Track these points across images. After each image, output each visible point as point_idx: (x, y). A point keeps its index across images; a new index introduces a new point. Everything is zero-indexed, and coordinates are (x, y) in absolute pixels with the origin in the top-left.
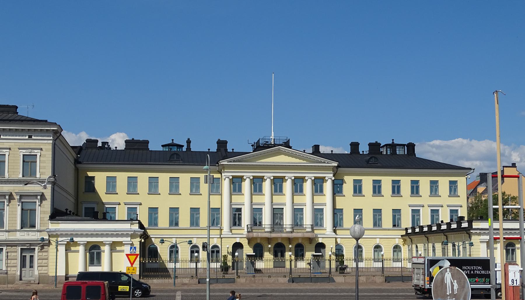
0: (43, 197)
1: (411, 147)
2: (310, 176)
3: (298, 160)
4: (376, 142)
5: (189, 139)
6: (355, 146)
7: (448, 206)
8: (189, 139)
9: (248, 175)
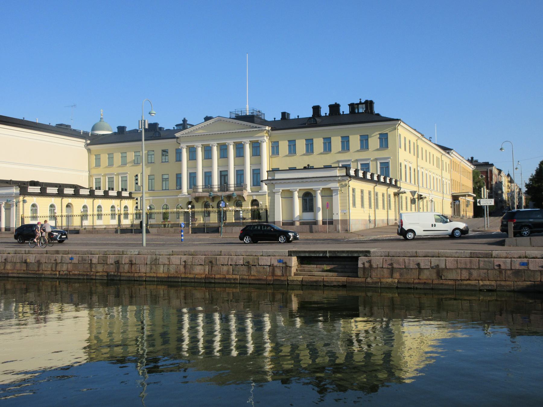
1: (369, 104)
4: (336, 103)
5: (184, 119)
6: (316, 109)
8: (184, 119)
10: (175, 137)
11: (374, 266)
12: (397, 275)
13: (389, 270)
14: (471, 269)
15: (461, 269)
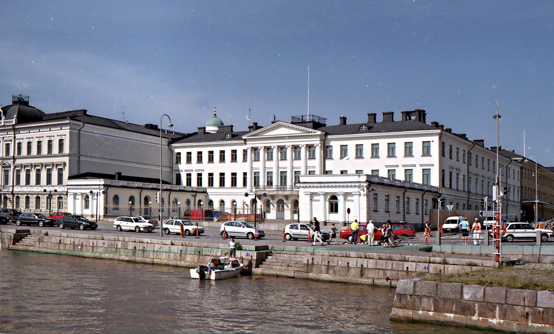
0: (65, 164)
2: (302, 143)
3: (299, 132)
6: (373, 116)
7: (421, 165)
9: (261, 145)
10: (241, 139)
11: (315, 263)
12: (331, 271)
13: (326, 267)
14: (387, 270)
15: (379, 269)
